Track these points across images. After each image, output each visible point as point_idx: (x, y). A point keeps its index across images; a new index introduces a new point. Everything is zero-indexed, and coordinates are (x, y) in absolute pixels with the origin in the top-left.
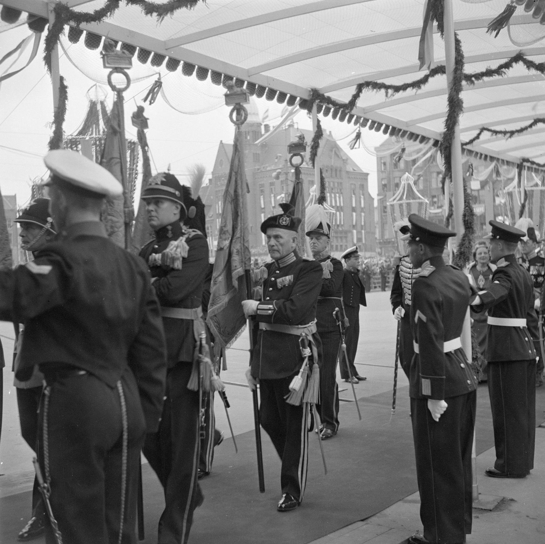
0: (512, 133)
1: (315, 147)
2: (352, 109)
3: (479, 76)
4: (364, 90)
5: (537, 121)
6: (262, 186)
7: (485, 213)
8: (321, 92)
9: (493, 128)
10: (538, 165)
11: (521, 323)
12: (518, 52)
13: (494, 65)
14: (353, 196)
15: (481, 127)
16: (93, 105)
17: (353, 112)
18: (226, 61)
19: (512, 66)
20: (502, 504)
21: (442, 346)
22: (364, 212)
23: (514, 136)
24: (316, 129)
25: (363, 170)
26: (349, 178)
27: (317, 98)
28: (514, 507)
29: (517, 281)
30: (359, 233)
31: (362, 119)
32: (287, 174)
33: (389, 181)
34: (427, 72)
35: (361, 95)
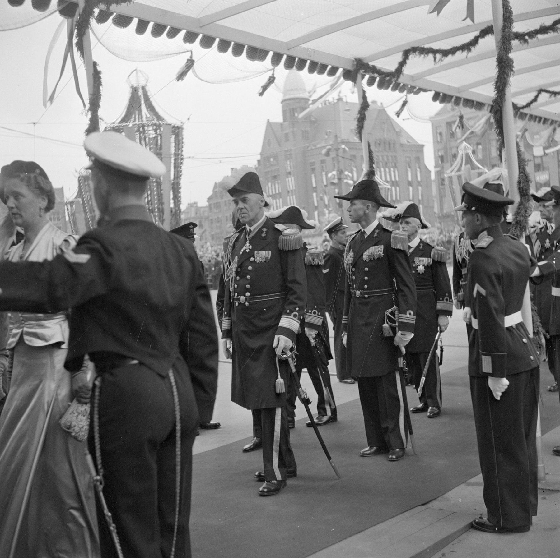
1: (361, 119)
2: (398, 77)
3: (532, 34)
4: (411, 57)
6: (313, 164)
8: (365, 62)
9: (551, 89)
14: (409, 169)
15: (539, 89)
16: (135, 90)
17: (402, 80)
18: (264, 36)
21: (503, 321)
22: (421, 186)
24: (362, 101)
25: (418, 141)
26: (403, 150)
27: (361, 68)
32: (337, 150)
33: (446, 153)
34: (477, 33)
35: (407, 61)
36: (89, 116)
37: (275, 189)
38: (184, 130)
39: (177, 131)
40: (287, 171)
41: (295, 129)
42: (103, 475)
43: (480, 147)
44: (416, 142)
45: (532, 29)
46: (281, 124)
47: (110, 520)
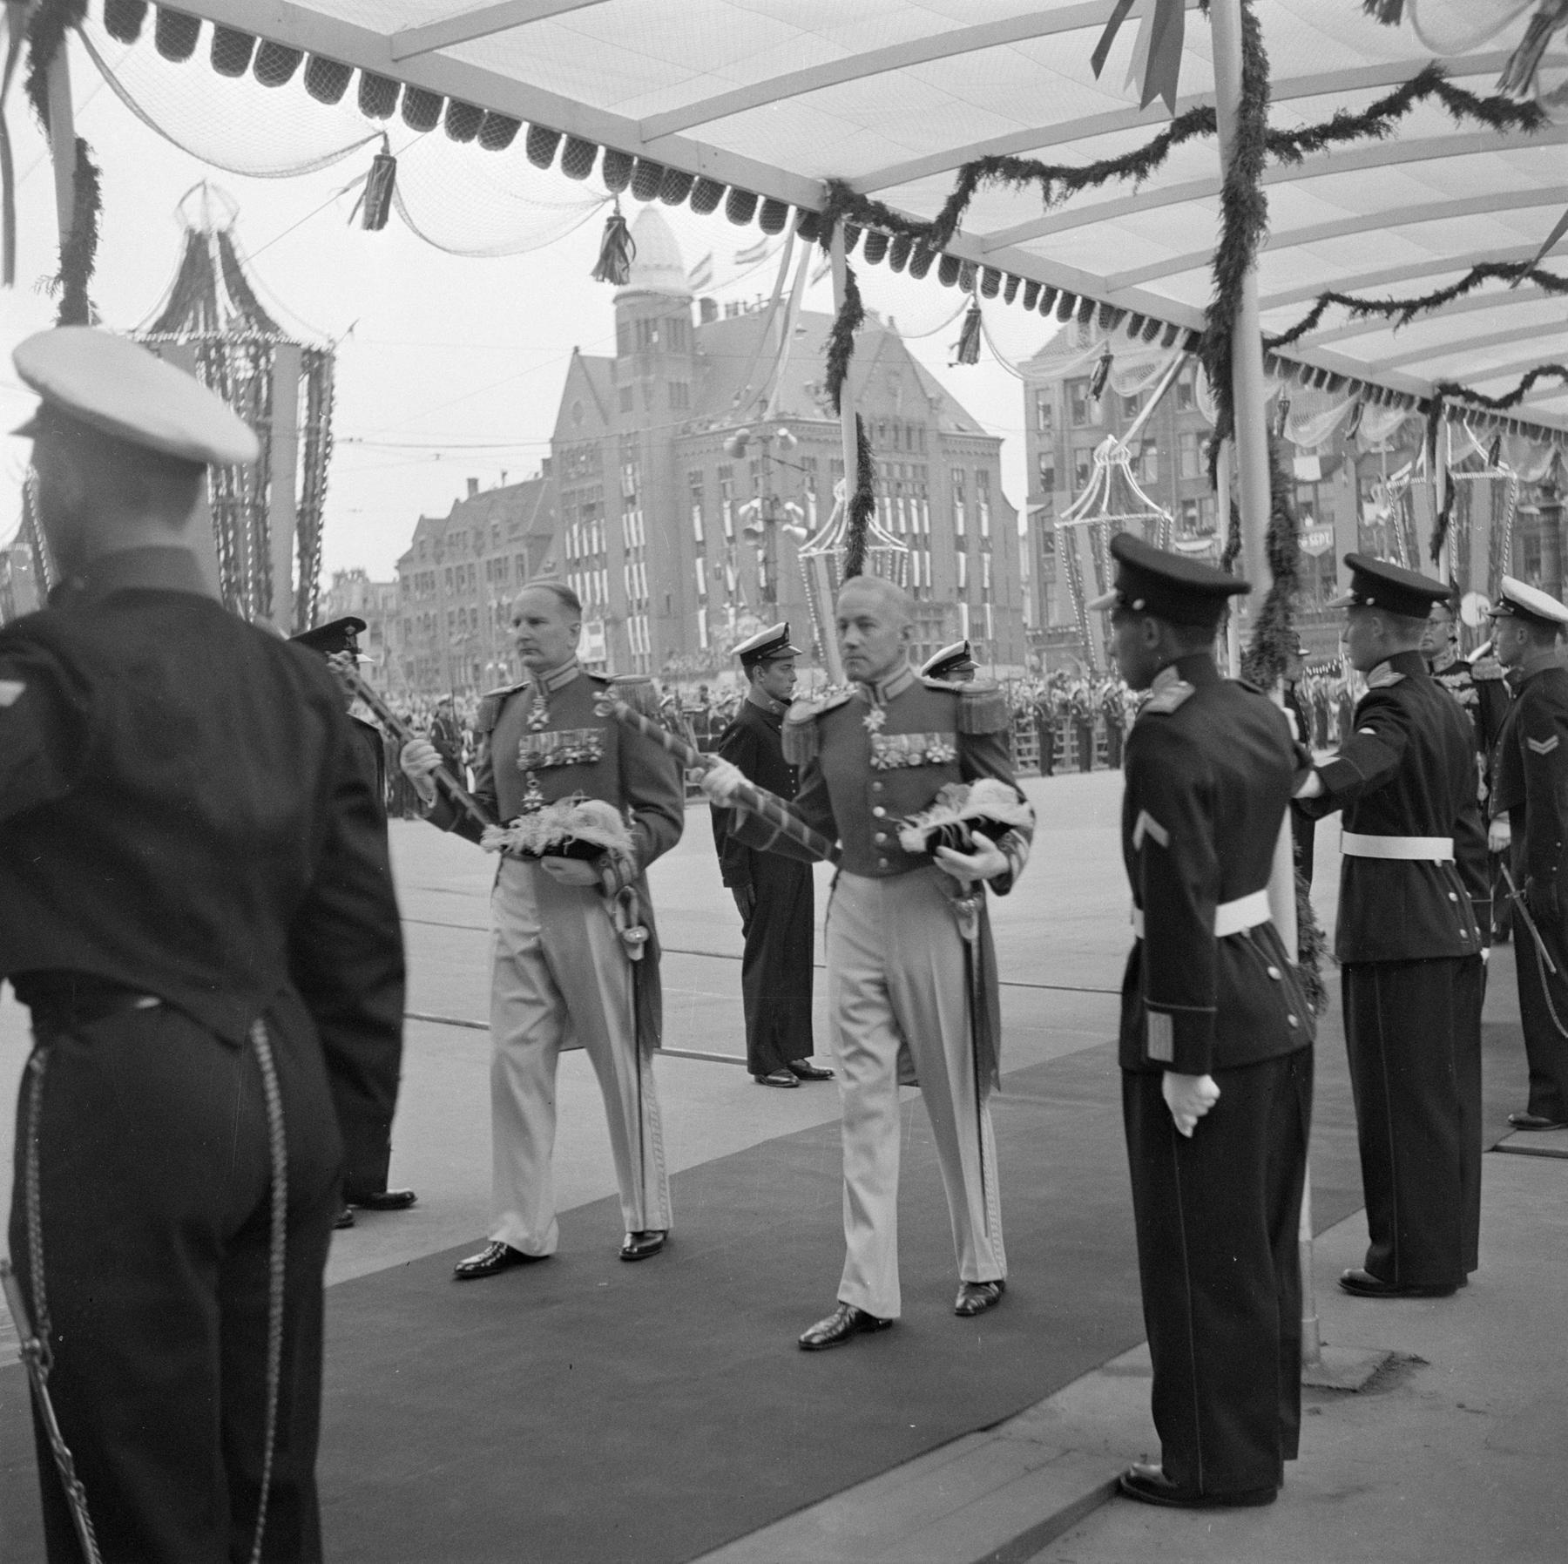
0: (1410, 308)
1: (841, 351)
2: (946, 239)
3: (1315, 137)
5: (1481, 272)
6: (697, 476)
7: (1333, 548)
8: (857, 191)
9: (1355, 295)
10: (1486, 401)
11: (1438, 849)
12: (1424, 66)
13: (1357, 104)
15: (1321, 292)
16: (196, 244)
17: (953, 248)
18: (574, 98)
19: (1408, 108)
20: (1389, 1372)
21: (1211, 918)
22: (990, 551)
23: (1415, 317)
24: (844, 299)
25: (983, 426)
26: (946, 452)
27: (844, 209)
28: (1422, 1380)
29: (1424, 727)
30: (976, 610)
31: (981, 269)
32: (766, 440)
33: (1060, 461)
34: (1164, 127)
35: (973, 197)
36: (60, 295)
37: (590, 542)
38: (336, 364)
39: (317, 364)
40: (626, 494)
41: (652, 378)
42: (52, 1338)
43: (1153, 451)
44: (981, 430)
45: (1312, 122)
46: (613, 363)
47: (66, 1469)
